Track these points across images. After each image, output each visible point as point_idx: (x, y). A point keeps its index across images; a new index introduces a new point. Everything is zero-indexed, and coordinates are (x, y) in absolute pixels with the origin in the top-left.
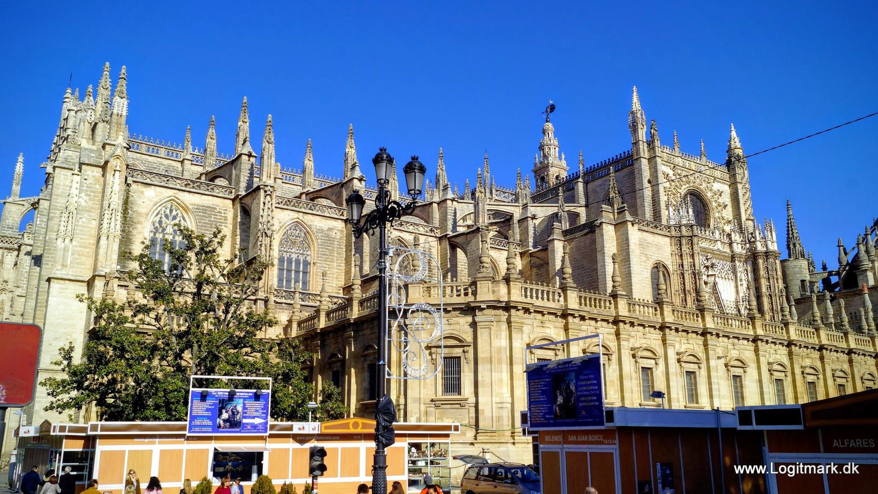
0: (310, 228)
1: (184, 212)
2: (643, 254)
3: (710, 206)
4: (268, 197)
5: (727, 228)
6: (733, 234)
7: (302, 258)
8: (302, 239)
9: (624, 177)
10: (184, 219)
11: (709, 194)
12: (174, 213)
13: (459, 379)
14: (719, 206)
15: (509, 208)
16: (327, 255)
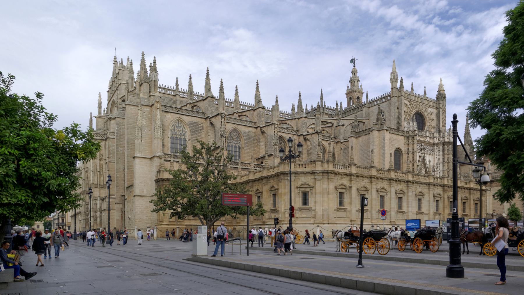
0: (240, 131)
1: (184, 125)
2: (391, 144)
3: (426, 119)
4: (223, 119)
5: (433, 130)
6: (435, 134)
7: (237, 146)
8: (237, 137)
9: (386, 105)
10: (184, 128)
11: (426, 114)
12: (180, 125)
13: (308, 200)
14: (430, 119)
15: (330, 120)
16: (248, 144)
